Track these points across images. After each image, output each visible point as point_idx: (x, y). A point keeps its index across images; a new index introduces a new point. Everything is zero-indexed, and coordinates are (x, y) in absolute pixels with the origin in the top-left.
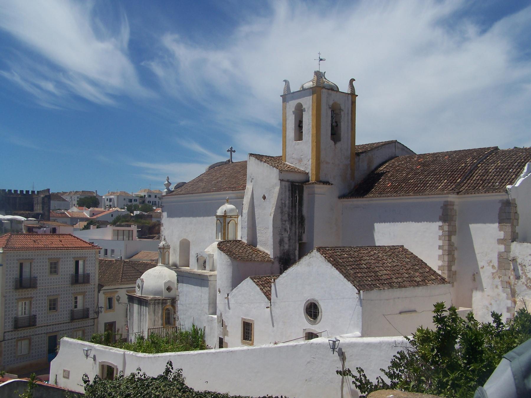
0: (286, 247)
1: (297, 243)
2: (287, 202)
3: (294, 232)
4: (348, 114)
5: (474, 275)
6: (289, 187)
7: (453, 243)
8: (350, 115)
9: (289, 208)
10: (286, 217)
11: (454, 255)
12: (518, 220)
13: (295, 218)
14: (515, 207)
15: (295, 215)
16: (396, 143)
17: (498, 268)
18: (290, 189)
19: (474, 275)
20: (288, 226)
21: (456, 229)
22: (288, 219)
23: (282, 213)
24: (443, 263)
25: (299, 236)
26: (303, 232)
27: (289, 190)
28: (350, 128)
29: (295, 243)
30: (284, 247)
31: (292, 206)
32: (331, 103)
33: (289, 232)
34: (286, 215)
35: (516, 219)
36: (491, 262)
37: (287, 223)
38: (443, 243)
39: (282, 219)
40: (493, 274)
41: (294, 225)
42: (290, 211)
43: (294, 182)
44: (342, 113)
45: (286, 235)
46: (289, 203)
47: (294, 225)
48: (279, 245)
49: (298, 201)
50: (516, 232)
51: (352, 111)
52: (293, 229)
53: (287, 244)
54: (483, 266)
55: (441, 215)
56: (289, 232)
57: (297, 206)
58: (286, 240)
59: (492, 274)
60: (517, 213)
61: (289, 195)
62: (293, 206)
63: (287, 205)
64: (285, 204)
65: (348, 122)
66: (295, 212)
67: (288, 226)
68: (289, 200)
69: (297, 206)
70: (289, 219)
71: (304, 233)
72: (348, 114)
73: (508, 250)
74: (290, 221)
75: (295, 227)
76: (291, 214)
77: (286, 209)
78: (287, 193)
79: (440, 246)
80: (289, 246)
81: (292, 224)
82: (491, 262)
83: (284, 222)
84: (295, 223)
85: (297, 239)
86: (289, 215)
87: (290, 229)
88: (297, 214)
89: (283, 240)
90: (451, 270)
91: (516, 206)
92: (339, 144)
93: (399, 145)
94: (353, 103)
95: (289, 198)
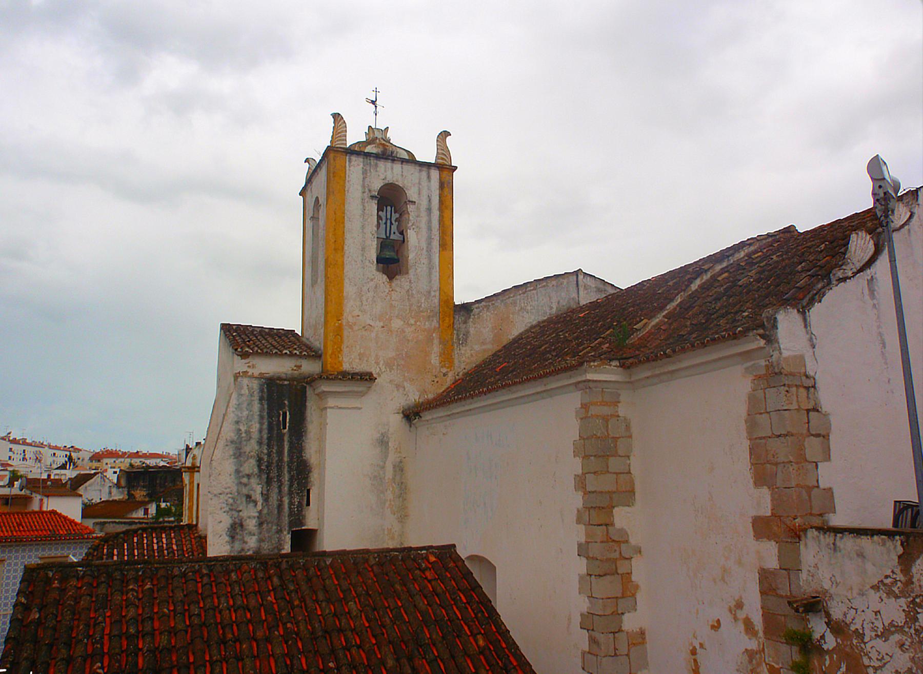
0: (252, 543)
1: (285, 533)
2: (255, 427)
3: (276, 503)
4: (429, 210)
5: (694, 652)
6: (262, 391)
7: (623, 532)
8: (436, 213)
9: (260, 443)
10: (250, 466)
11: (630, 574)
12: (826, 437)
13: (280, 468)
14: (807, 388)
15: (281, 460)
16: (581, 277)
17: (765, 633)
18: (265, 396)
19: (694, 652)
20: (259, 489)
21: (632, 482)
22: (256, 470)
23: (239, 454)
24: (589, 605)
25: (291, 513)
26: (305, 502)
27: (261, 399)
28: (436, 244)
29: (279, 531)
30: (246, 543)
31: (269, 439)
32: (377, 185)
33: (259, 504)
34: (253, 462)
35: (818, 435)
36: (739, 605)
37: (254, 481)
38: (587, 535)
39: (237, 471)
40: (750, 654)
41: (275, 485)
42: (265, 451)
43: (280, 379)
44: (411, 208)
45: (250, 514)
46: (261, 431)
47: (275, 485)
48: (227, 539)
49: (287, 425)
50: (822, 486)
51: (441, 202)
52: (274, 496)
53: (254, 535)
54: (718, 621)
55: (578, 438)
56: (259, 504)
57: (286, 438)
58: (251, 525)
59: (746, 658)
60: (815, 410)
61: (261, 411)
62: (273, 436)
63: (255, 435)
64: (248, 432)
65: (430, 229)
66: (280, 453)
67: (257, 489)
68: (261, 424)
69: (286, 438)
70: (260, 470)
71: (308, 504)
72: (429, 210)
73: (791, 566)
74: (264, 477)
75: (280, 491)
76: (266, 459)
77: (252, 447)
78: (256, 406)
79: (580, 545)
80: (261, 540)
81: (269, 482)
82: (739, 605)
83: (245, 480)
84: (280, 481)
85: (286, 520)
86: (260, 461)
87: (266, 497)
88: (286, 459)
89: (241, 525)
90: (620, 631)
91: (809, 383)
92: (401, 282)
93: (588, 281)
94: (446, 187)
95: (261, 417)
